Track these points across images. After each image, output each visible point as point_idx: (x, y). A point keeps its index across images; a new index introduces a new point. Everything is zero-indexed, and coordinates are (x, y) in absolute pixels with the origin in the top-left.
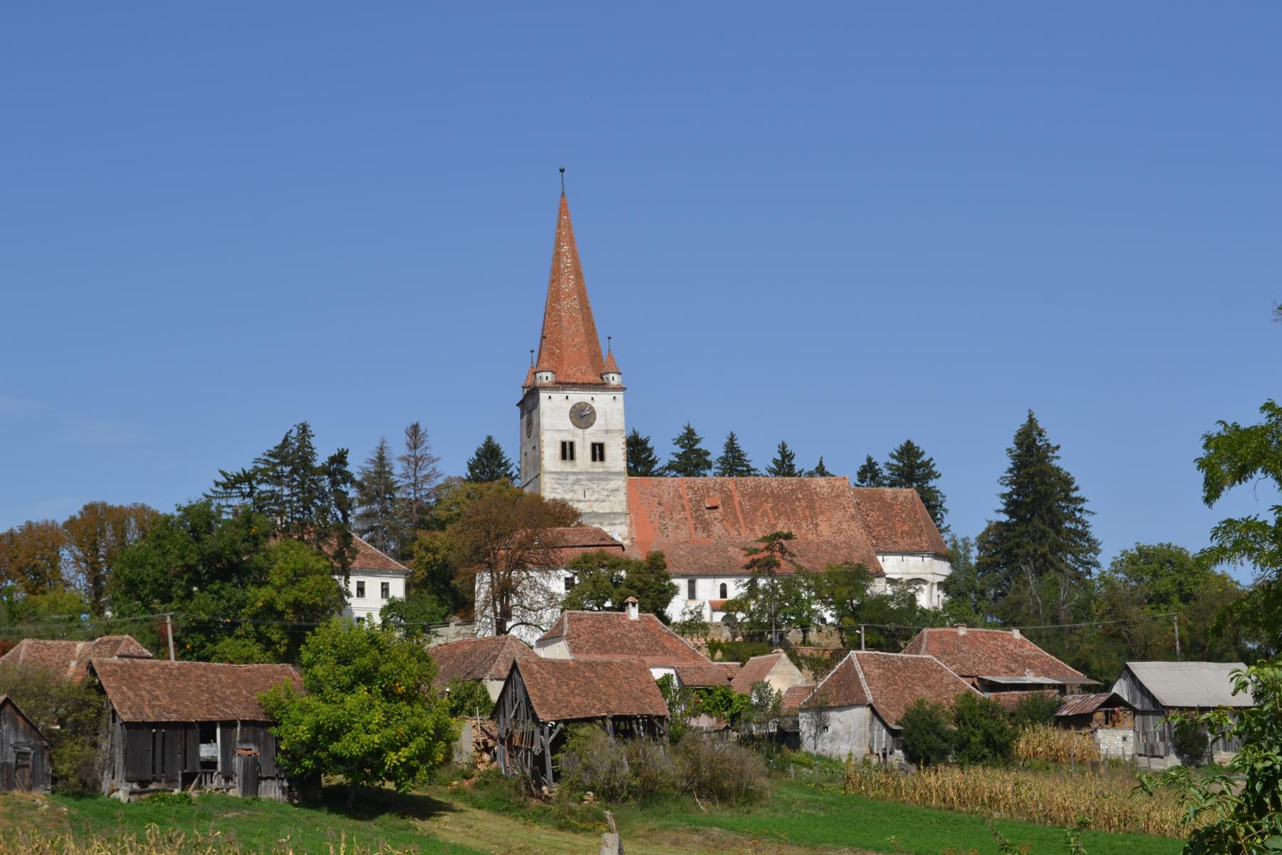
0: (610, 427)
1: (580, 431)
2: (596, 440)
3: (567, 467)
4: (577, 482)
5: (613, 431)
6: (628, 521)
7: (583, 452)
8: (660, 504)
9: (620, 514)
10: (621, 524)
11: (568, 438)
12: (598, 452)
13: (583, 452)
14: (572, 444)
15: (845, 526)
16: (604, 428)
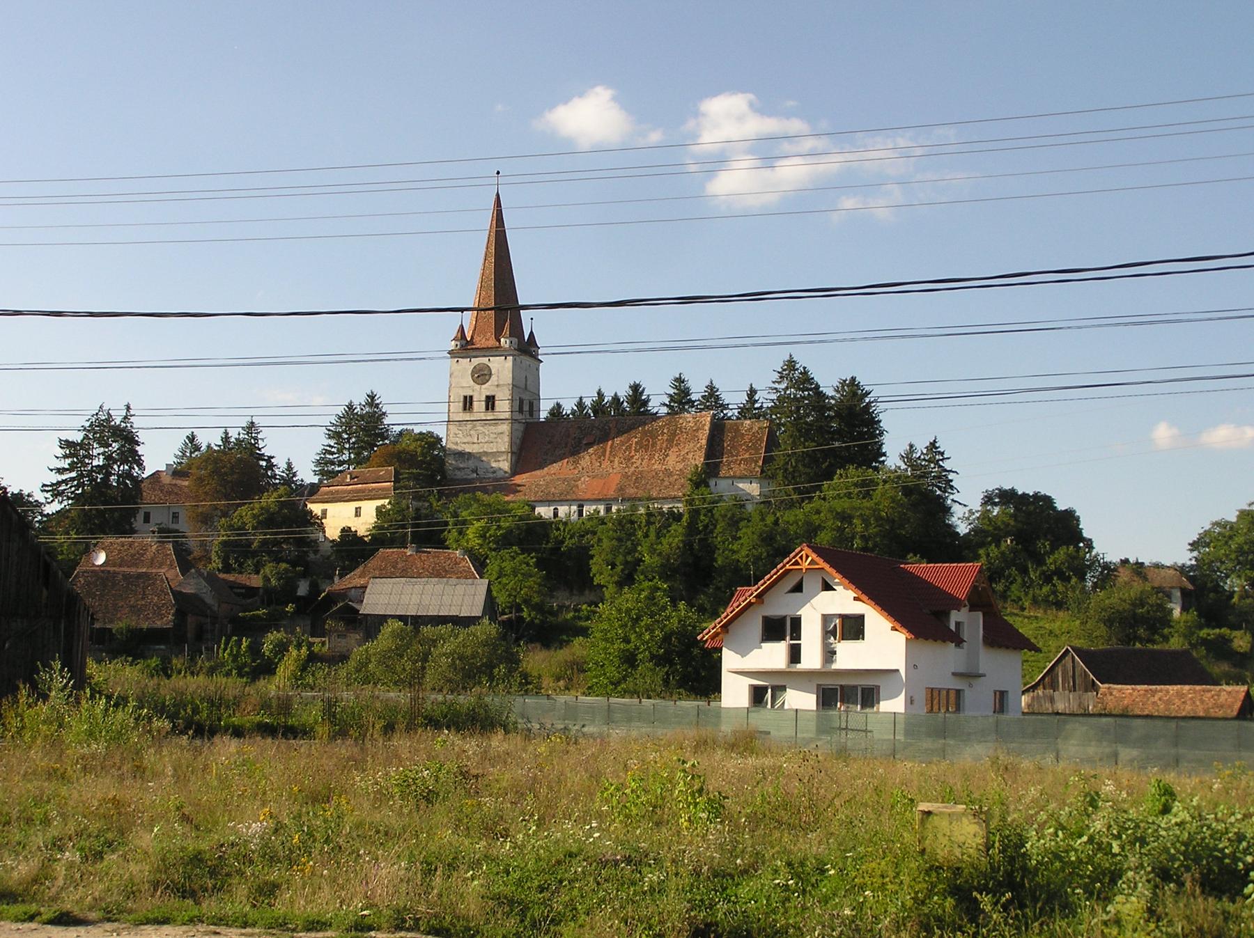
0: (501, 383)
1: (477, 387)
2: (488, 394)
3: (467, 416)
4: (475, 426)
5: (504, 385)
6: (509, 458)
7: (479, 406)
8: (549, 443)
9: (504, 452)
10: (504, 460)
11: (469, 393)
12: (490, 402)
13: (479, 406)
14: (471, 397)
15: (690, 456)
16: (496, 383)
